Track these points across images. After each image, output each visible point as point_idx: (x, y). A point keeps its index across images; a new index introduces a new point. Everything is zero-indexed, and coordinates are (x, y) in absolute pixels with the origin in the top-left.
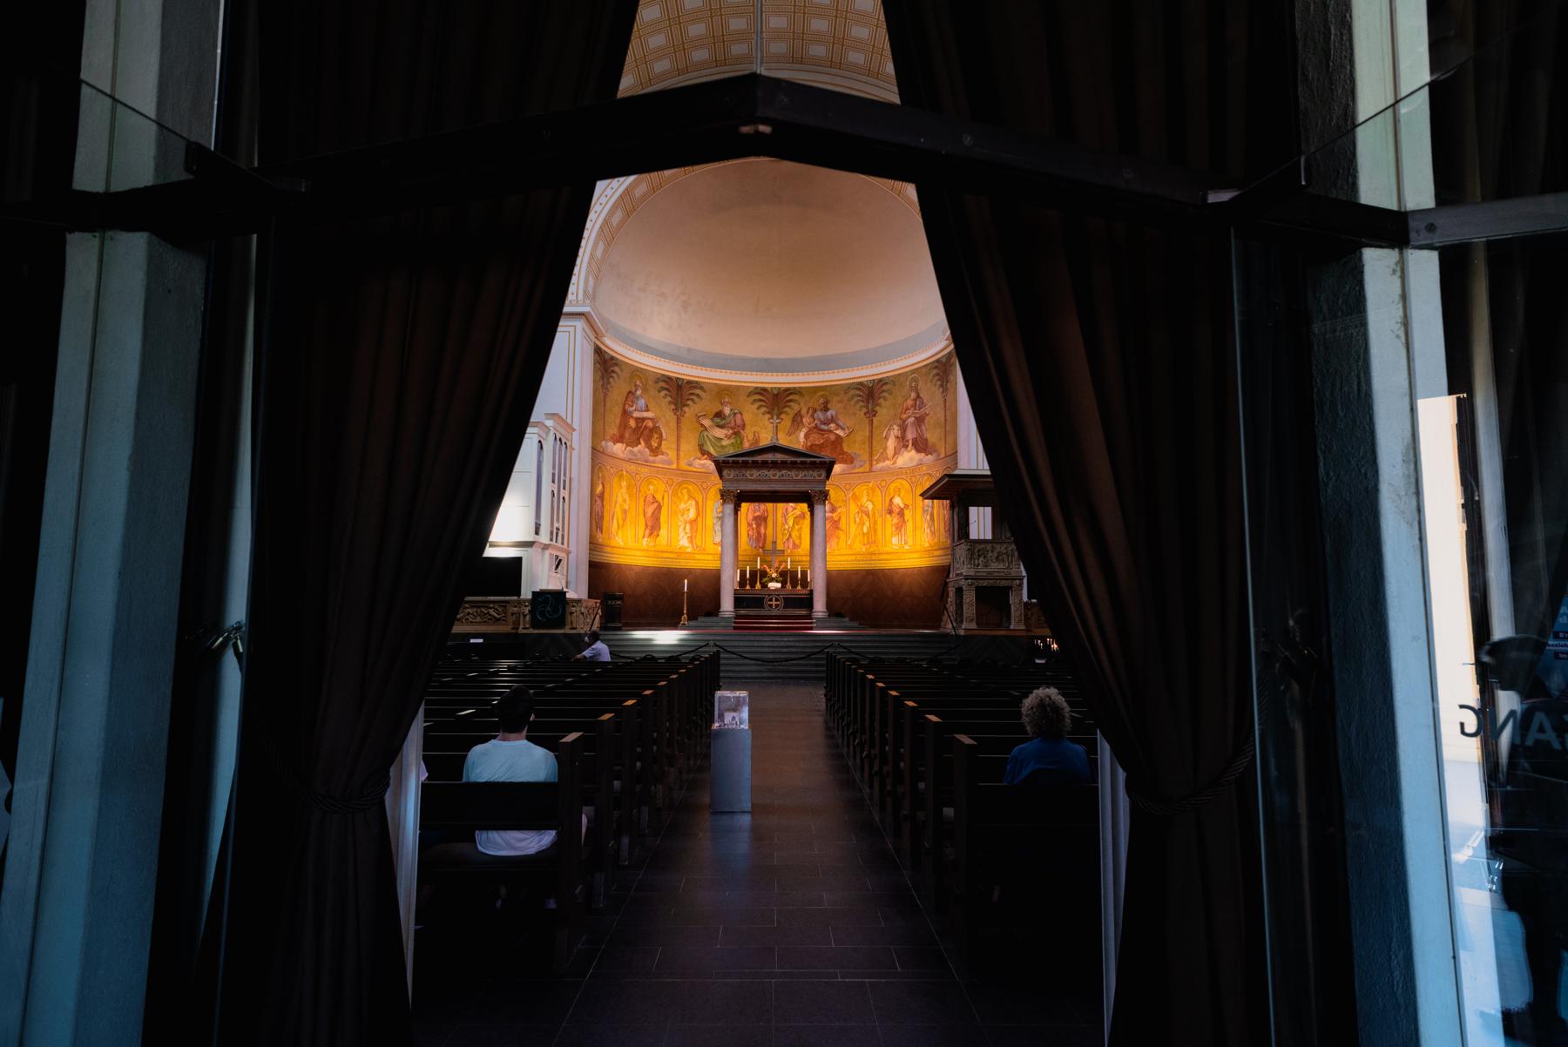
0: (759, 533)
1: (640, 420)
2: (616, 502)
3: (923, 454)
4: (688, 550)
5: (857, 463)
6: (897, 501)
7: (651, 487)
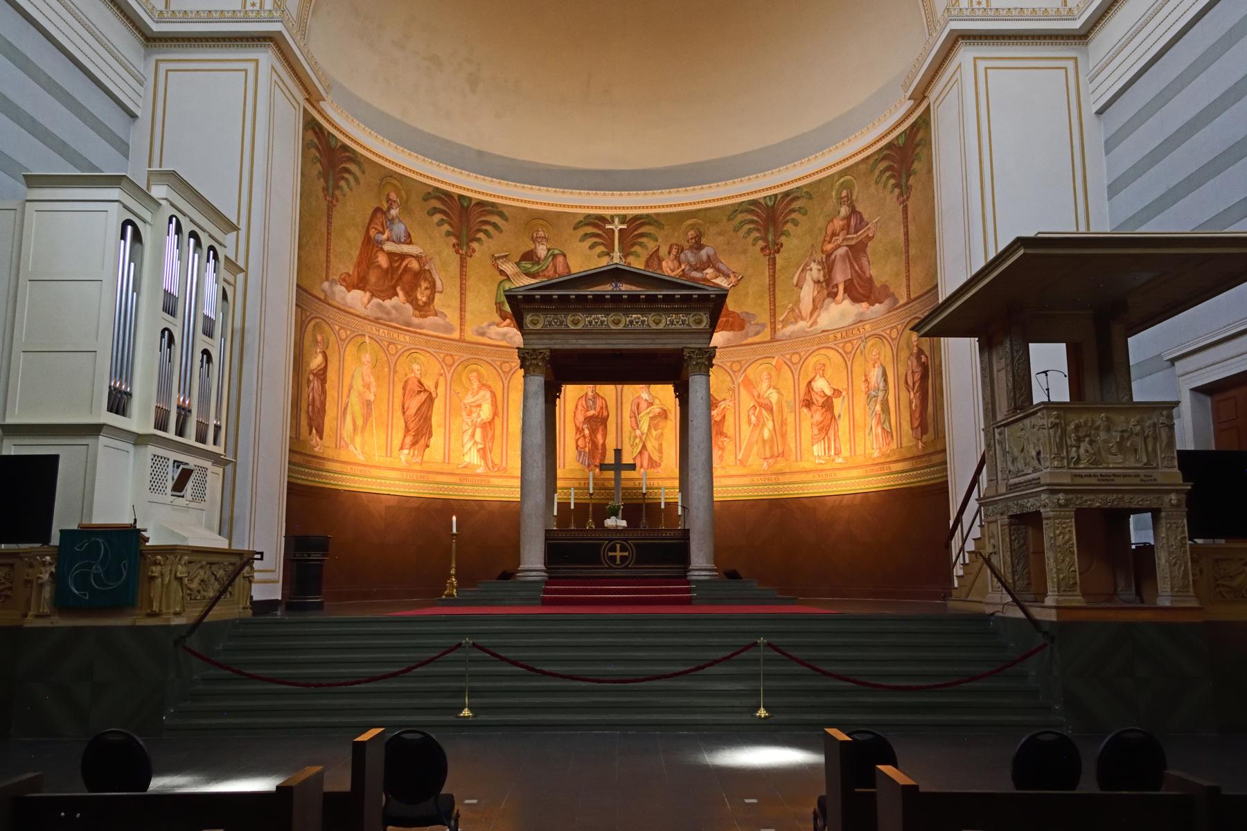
0: (594, 444)
2: (351, 388)
3: (864, 305)
4: (479, 471)
5: (750, 329)
6: (821, 385)
7: (416, 367)
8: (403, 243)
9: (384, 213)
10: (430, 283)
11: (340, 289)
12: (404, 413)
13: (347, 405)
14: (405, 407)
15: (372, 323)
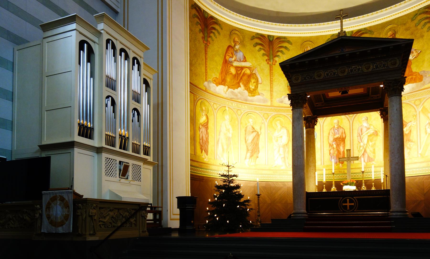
0: (339, 152)
1: (239, 69)
8: (242, 62)
9: (233, 48)
10: (256, 80)
12: (246, 142)
13: (219, 139)
14: (247, 139)
15: (229, 101)
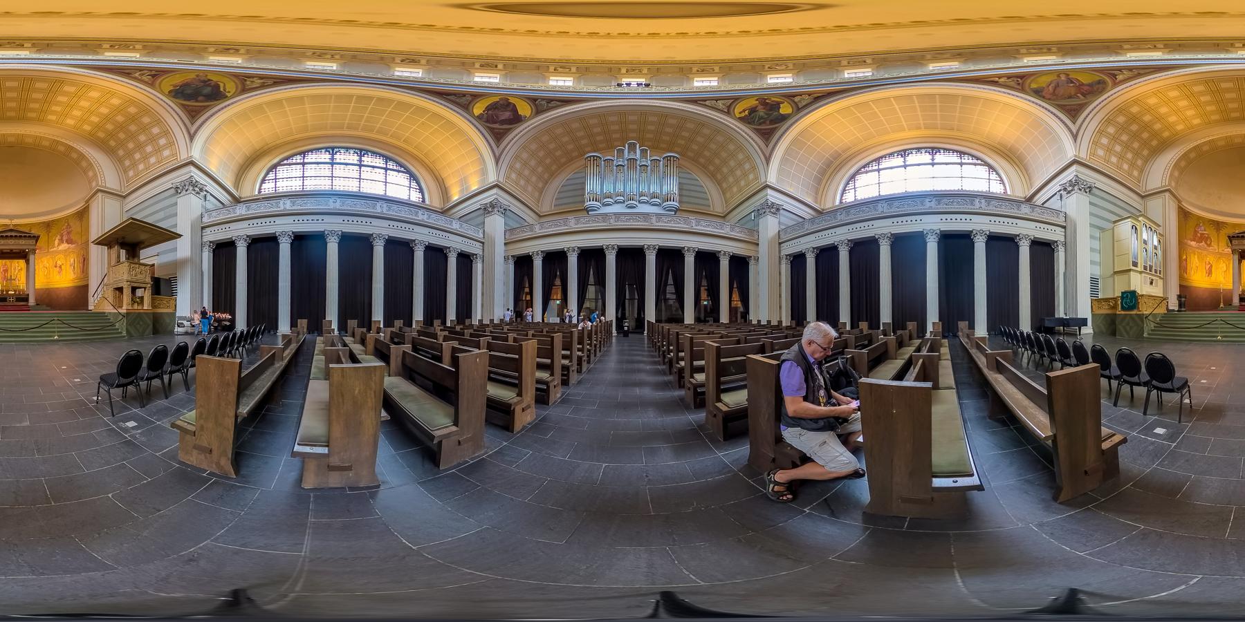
11: (1189, 241)
